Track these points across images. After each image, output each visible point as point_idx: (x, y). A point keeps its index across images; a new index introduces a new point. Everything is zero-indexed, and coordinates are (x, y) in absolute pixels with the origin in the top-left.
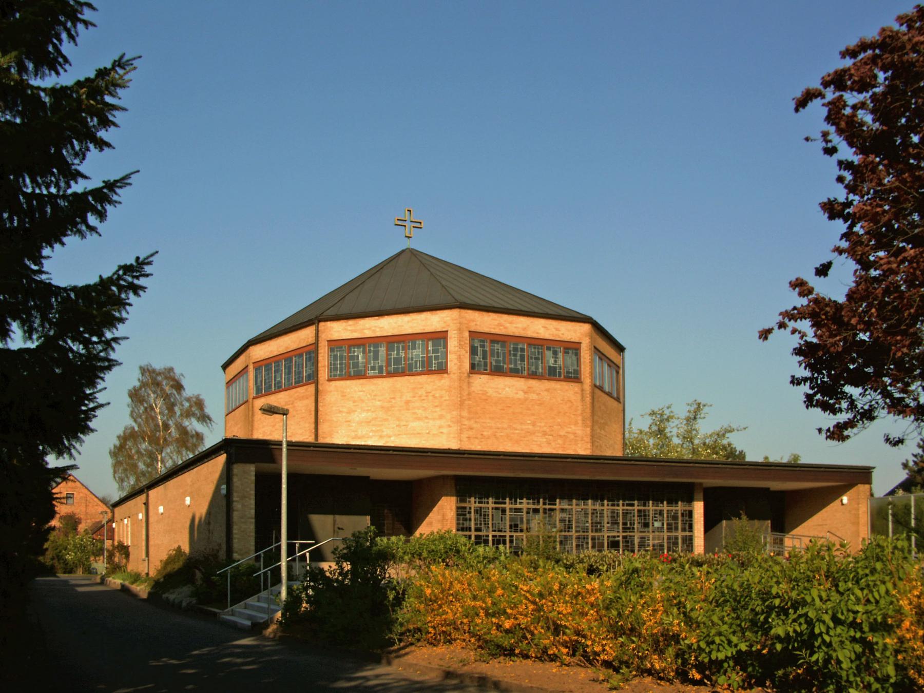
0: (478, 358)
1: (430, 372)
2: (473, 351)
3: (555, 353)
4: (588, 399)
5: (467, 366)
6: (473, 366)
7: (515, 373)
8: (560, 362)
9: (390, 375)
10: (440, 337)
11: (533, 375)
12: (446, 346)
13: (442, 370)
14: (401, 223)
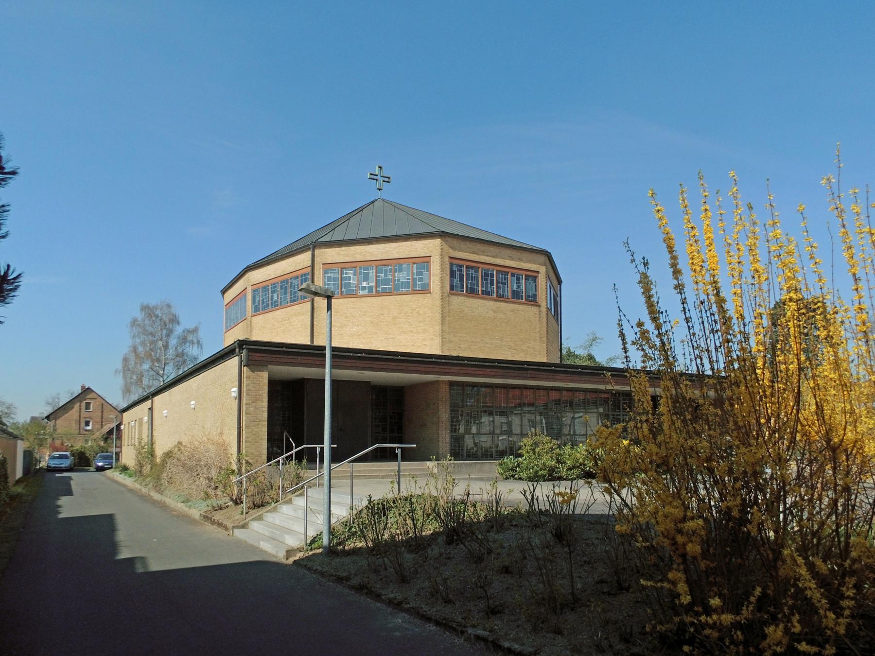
0: (456, 281)
1: (415, 292)
2: (452, 274)
3: (518, 279)
5: (448, 287)
6: (452, 288)
9: (379, 294)
10: (423, 262)
11: (501, 297)
12: (428, 270)
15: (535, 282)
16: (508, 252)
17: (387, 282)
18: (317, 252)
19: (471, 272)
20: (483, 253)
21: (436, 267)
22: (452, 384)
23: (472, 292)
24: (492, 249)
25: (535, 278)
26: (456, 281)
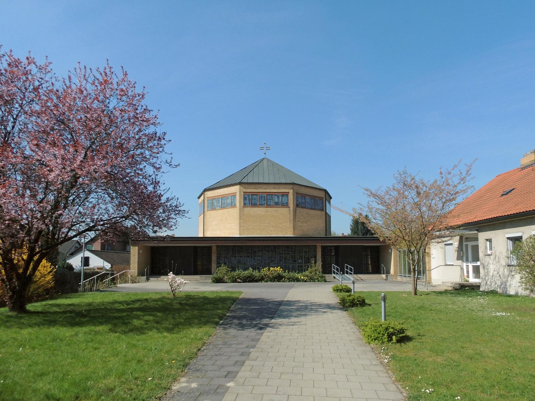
2: (245, 199)
3: (278, 197)
4: (292, 213)
5: (242, 204)
6: (245, 204)
7: (261, 205)
8: (280, 200)
10: (234, 195)
11: (269, 206)
13: (235, 206)
14: (262, 148)
15: (287, 197)
16: (273, 186)
17: (225, 203)
18: (205, 193)
19: (254, 197)
20: (260, 188)
22: (217, 246)
23: (254, 205)
24: (265, 186)
25: (287, 195)
26: (247, 201)
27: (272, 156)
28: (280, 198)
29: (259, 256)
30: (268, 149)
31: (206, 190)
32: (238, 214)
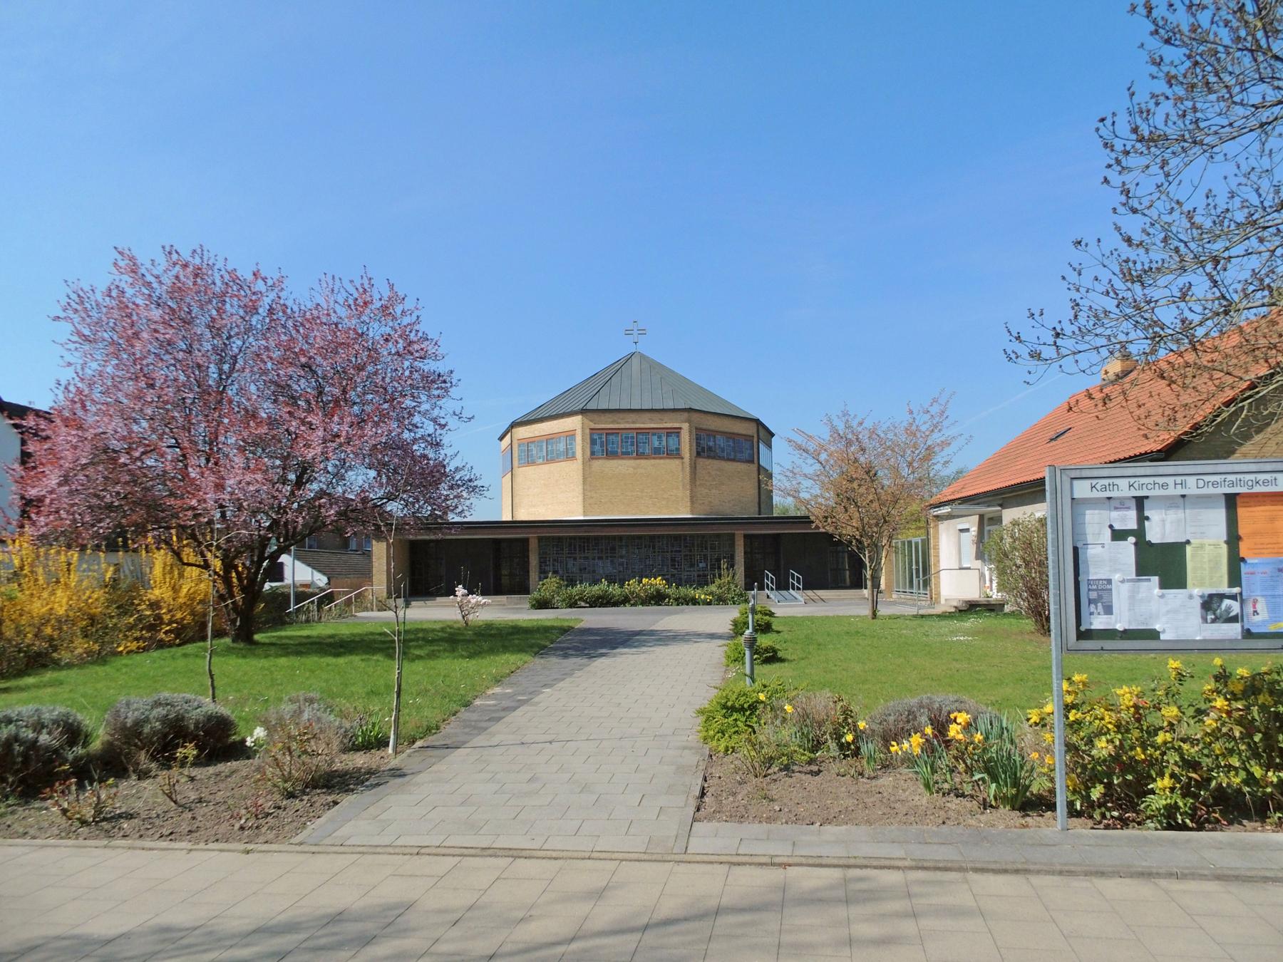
0: (597, 447)
2: (593, 442)
3: (659, 437)
4: (688, 469)
5: (588, 453)
6: (593, 453)
7: (626, 455)
10: (570, 435)
11: (640, 456)
13: (573, 457)
14: (628, 332)
16: (648, 415)
17: (552, 451)
19: (611, 437)
21: (579, 438)
23: (611, 455)
26: (597, 447)
27: (650, 348)
28: (664, 439)
29: (622, 557)
30: (642, 332)
31: (514, 425)
32: (580, 472)
